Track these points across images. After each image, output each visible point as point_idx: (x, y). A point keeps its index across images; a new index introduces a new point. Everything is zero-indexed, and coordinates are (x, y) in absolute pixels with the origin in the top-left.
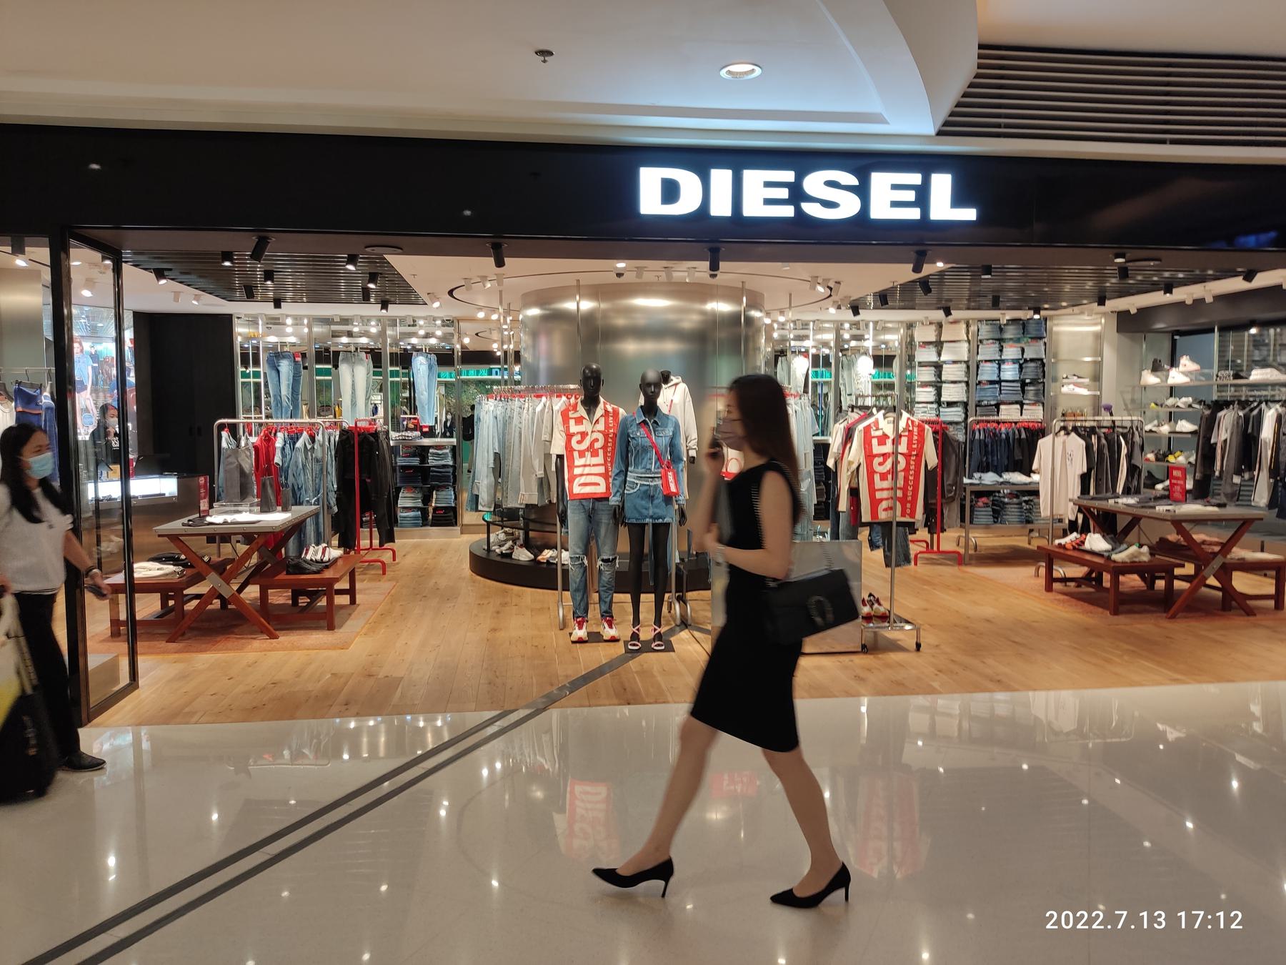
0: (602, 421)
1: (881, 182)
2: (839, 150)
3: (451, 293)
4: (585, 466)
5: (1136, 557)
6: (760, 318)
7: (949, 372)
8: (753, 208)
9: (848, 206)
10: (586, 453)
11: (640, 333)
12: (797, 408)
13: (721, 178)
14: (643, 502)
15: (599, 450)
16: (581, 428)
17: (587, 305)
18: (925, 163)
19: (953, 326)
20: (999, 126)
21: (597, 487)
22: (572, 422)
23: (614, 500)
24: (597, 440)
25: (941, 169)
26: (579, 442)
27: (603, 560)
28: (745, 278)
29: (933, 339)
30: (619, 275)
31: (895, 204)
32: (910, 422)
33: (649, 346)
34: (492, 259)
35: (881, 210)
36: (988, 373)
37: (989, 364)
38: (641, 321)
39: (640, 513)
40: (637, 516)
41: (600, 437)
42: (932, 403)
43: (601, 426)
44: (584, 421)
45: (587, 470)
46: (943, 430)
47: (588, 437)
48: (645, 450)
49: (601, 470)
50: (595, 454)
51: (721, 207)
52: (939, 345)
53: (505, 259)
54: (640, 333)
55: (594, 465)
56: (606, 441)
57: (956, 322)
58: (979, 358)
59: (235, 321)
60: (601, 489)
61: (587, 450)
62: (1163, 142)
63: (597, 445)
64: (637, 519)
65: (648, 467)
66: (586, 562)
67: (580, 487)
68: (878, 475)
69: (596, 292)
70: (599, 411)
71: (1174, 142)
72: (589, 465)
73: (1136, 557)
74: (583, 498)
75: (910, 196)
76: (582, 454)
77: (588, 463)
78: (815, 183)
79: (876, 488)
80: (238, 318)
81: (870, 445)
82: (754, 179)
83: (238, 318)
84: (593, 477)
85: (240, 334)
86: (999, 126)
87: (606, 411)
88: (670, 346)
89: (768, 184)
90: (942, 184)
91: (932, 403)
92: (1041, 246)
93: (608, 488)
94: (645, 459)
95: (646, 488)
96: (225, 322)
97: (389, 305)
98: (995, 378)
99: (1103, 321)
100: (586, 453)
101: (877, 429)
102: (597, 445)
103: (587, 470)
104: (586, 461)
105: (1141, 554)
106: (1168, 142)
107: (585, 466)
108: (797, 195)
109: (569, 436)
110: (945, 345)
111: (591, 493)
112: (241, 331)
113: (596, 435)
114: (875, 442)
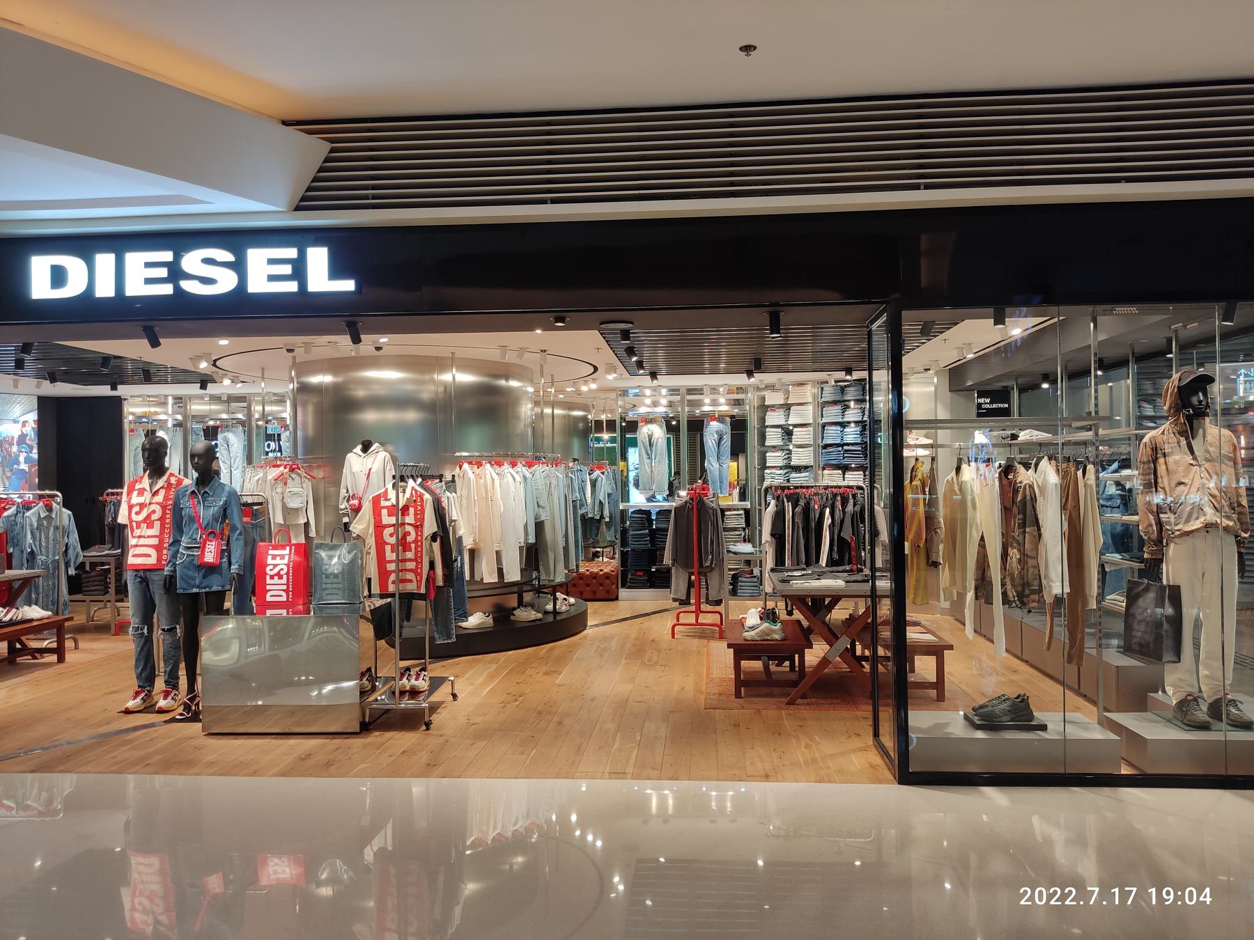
0: (162, 492)
1: (257, 258)
2: (161, 231)
3: (596, 369)
4: (140, 537)
5: (768, 635)
6: (519, 388)
7: (800, 435)
8: (136, 287)
9: (226, 282)
10: (142, 524)
11: (378, 402)
12: (572, 476)
13: (104, 261)
14: (190, 573)
15: (156, 522)
16: (141, 500)
17: (323, 379)
18: (301, 237)
19: (799, 388)
20: (367, 197)
21: (149, 558)
22: (135, 493)
23: (167, 570)
24: (154, 512)
25: (317, 243)
26: (137, 513)
27: (163, 630)
28: (453, 350)
29: (782, 402)
30: (378, 349)
31: (149, 281)
32: (414, 492)
33: (391, 416)
34: (349, 336)
35: (258, 284)
36: (832, 435)
37: (834, 428)
38: (380, 391)
39: (188, 584)
40: (184, 586)
41: (158, 508)
42: (781, 468)
43: (159, 498)
44: (145, 493)
45: (142, 541)
46: (700, 496)
47: (145, 510)
48: (192, 520)
49: (155, 541)
50: (150, 526)
51: (104, 289)
52: (787, 407)
53: (361, 336)
54: (378, 402)
55: (149, 537)
56: (164, 513)
57: (801, 384)
58: (825, 420)
59: (125, 403)
60: (152, 560)
61: (145, 520)
62: (543, 202)
63: (154, 517)
64: (184, 589)
65: (194, 537)
66: (145, 631)
67: (134, 558)
68: (390, 546)
69: (334, 365)
70: (161, 482)
71: (554, 201)
72: (144, 537)
73: (768, 635)
74: (137, 569)
75: (287, 269)
76: (139, 524)
77: (143, 534)
78: (192, 261)
79: (387, 559)
80: (125, 399)
81: (380, 515)
82: (135, 260)
83: (125, 399)
84: (146, 548)
85: (133, 414)
86: (367, 197)
87: (168, 481)
88: (411, 416)
89: (148, 265)
90: (318, 258)
91: (781, 468)
92: (170, 320)
93: (159, 560)
94: (192, 530)
95: (192, 558)
96: (117, 402)
97: (209, 384)
98: (838, 441)
99: (935, 380)
100: (142, 524)
101: (387, 500)
102: (154, 517)
103: (142, 541)
104: (141, 532)
105: (773, 631)
106: (549, 202)
107: (140, 537)
108: (176, 273)
109: (131, 507)
110: (792, 408)
111: (141, 565)
112: (132, 410)
113: (153, 507)
114: (384, 512)
